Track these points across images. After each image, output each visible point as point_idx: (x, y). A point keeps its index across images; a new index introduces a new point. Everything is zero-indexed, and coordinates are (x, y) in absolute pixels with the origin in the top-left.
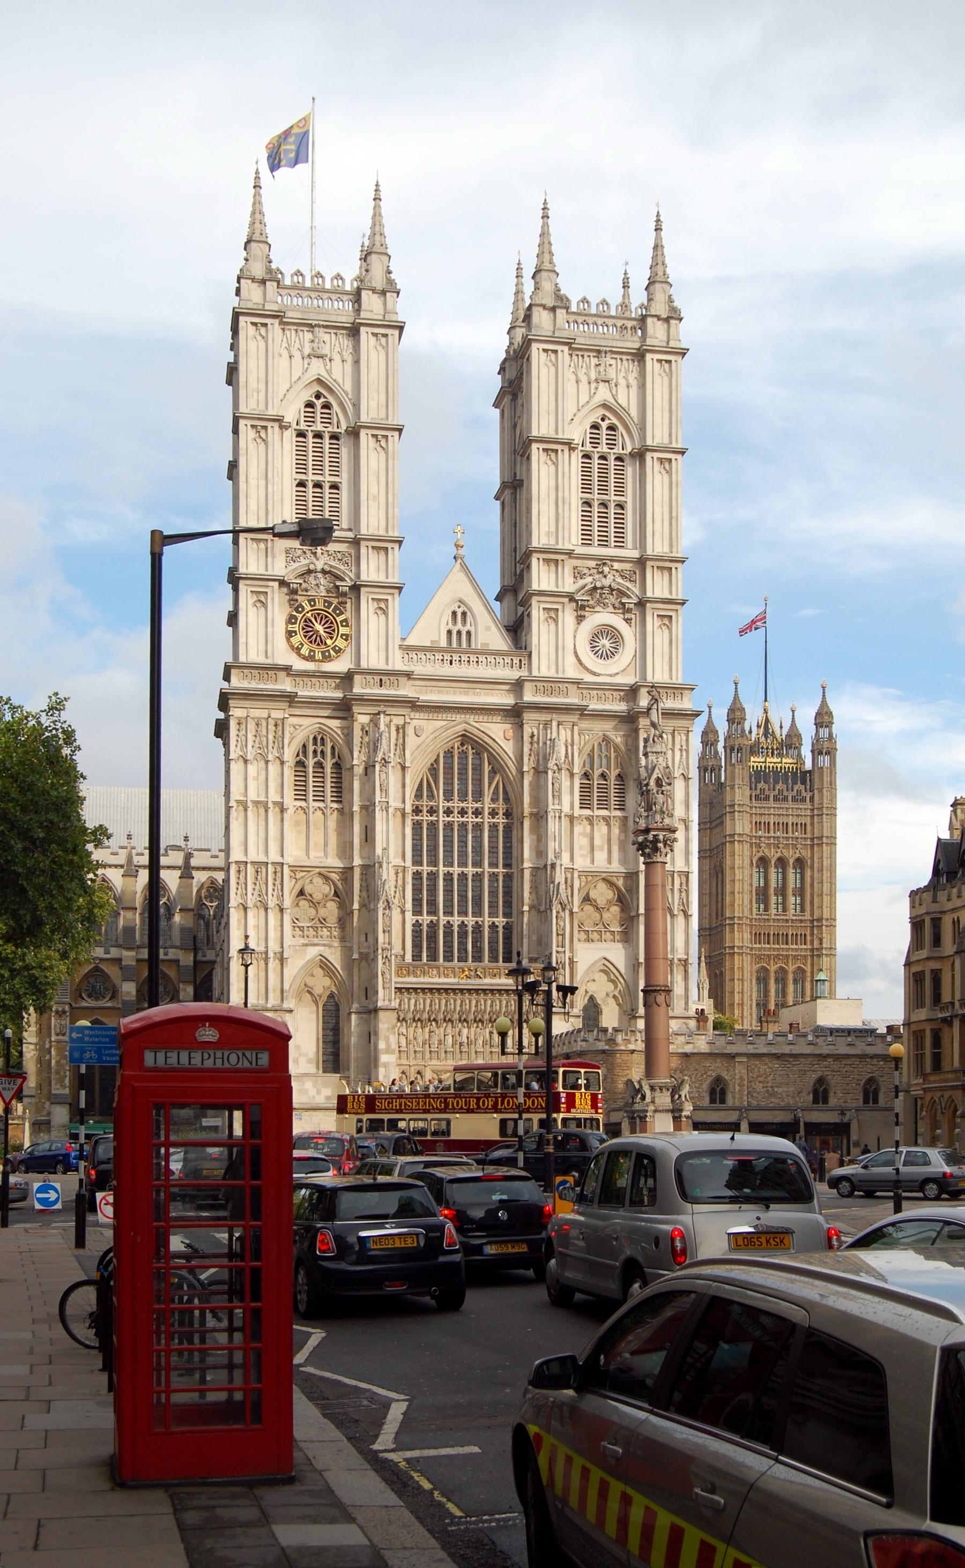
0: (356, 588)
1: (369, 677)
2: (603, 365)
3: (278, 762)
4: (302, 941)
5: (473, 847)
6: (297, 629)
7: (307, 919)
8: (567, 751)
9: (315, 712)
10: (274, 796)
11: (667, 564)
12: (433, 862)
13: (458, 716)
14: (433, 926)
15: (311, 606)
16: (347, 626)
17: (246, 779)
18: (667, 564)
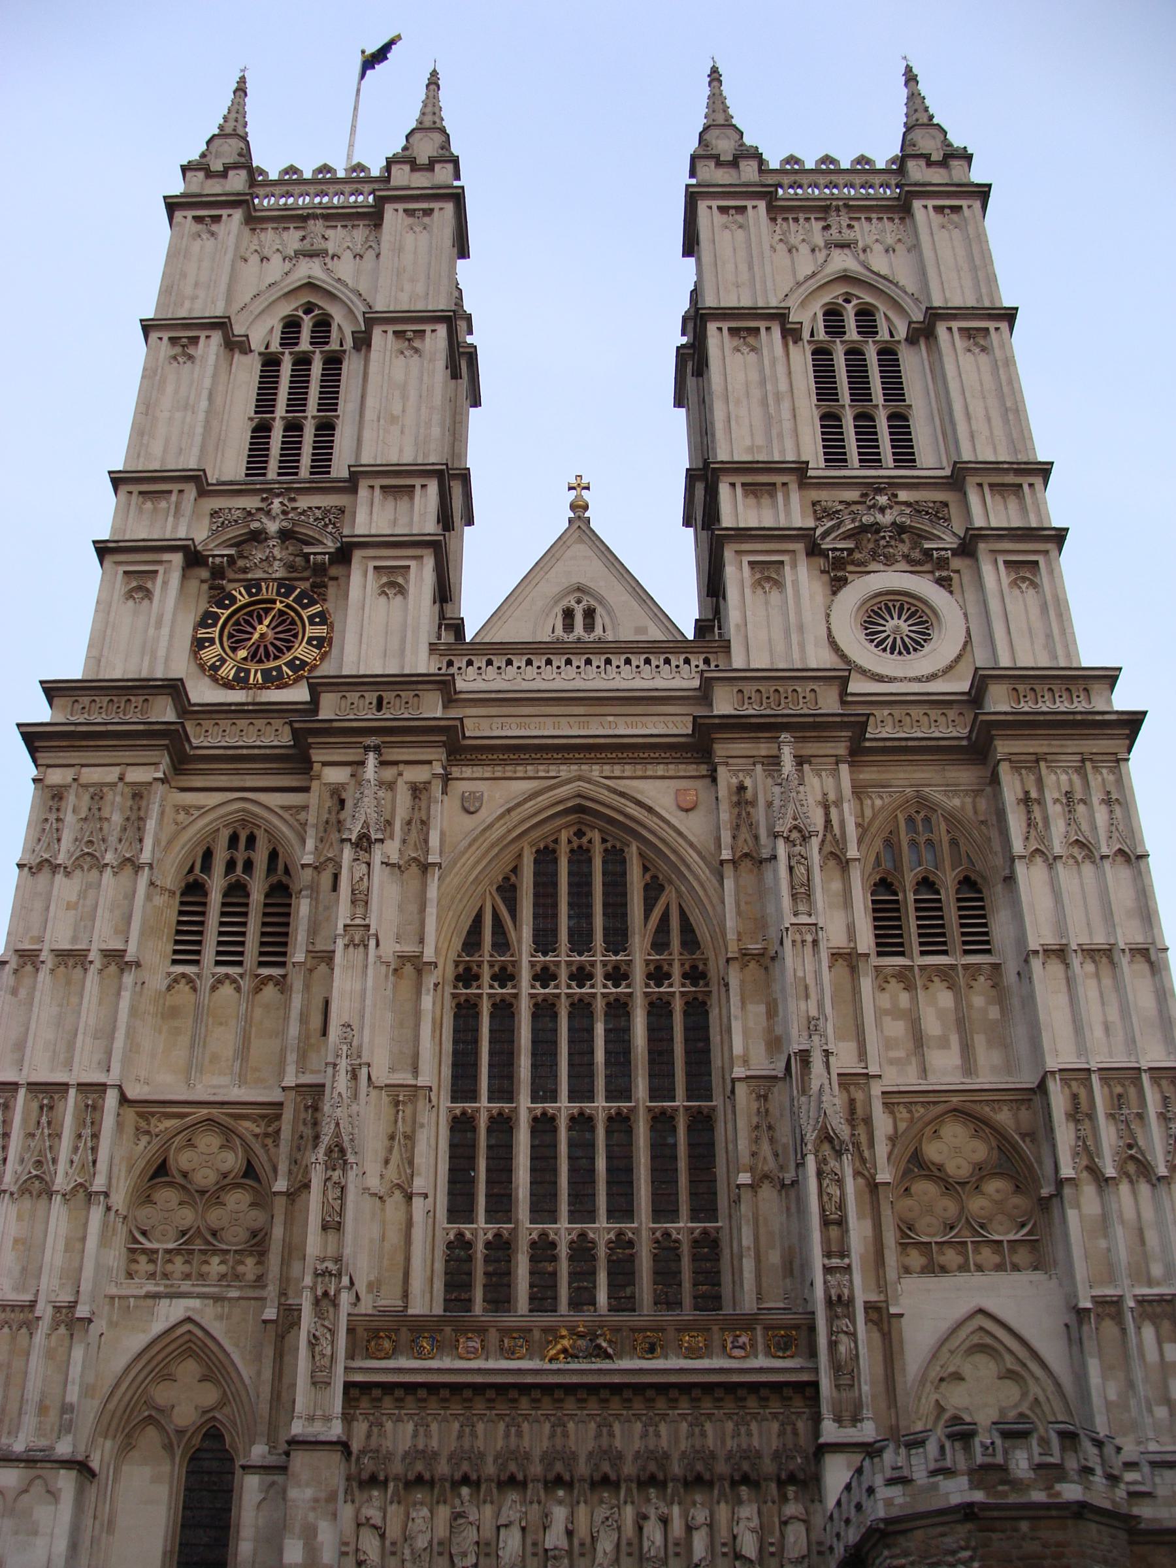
0: (344, 555)
1: (353, 696)
2: (833, 228)
3: (128, 870)
4: (151, 1287)
5: (607, 1052)
7: (172, 1233)
8: (827, 814)
9: (236, 782)
11: (1010, 479)
12: (504, 1089)
13: (563, 767)
14: (501, 1247)
15: (251, 595)
16: (324, 622)
17: (47, 908)
18: (1010, 479)
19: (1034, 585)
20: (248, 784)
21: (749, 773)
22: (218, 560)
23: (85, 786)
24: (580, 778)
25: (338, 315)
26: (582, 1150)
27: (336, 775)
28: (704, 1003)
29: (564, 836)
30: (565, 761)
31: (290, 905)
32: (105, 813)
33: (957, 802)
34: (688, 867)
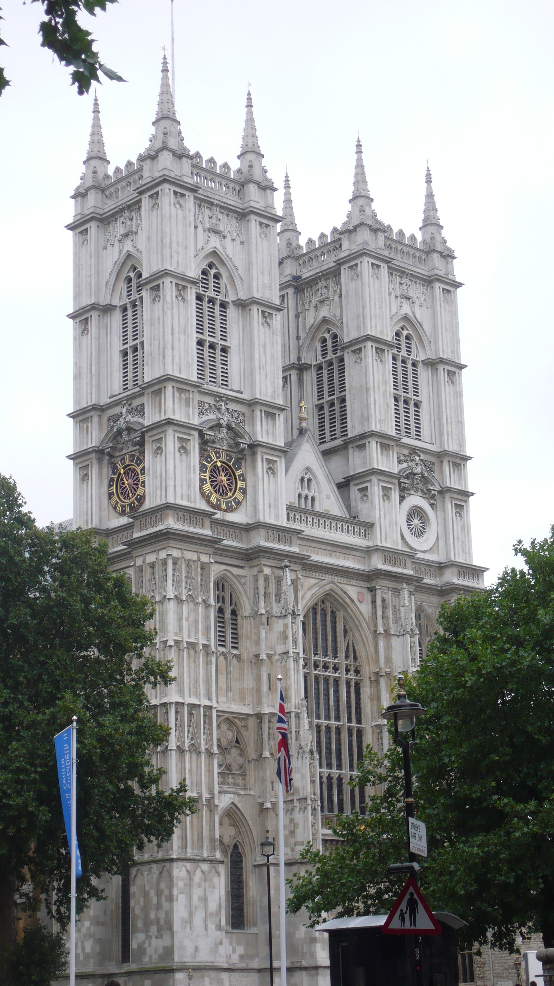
2: (405, 284)
6: (207, 478)
10: (202, 641)
11: (458, 461)
19: (460, 516)
20: (226, 562)
21: (385, 593)
22: (209, 437)
23: (185, 560)
24: (333, 583)
25: (224, 280)
26: (329, 739)
27: (267, 571)
28: (359, 684)
29: (320, 603)
30: (327, 573)
31: (236, 620)
32: (193, 576)
33: (430, 610)
34: (362, 628)
